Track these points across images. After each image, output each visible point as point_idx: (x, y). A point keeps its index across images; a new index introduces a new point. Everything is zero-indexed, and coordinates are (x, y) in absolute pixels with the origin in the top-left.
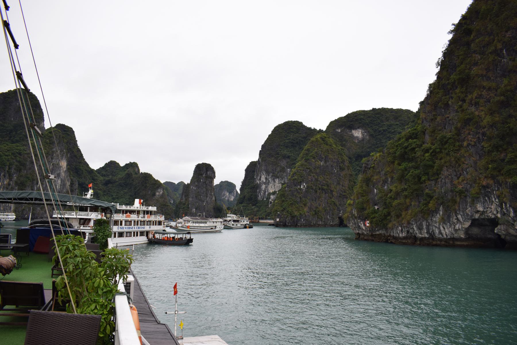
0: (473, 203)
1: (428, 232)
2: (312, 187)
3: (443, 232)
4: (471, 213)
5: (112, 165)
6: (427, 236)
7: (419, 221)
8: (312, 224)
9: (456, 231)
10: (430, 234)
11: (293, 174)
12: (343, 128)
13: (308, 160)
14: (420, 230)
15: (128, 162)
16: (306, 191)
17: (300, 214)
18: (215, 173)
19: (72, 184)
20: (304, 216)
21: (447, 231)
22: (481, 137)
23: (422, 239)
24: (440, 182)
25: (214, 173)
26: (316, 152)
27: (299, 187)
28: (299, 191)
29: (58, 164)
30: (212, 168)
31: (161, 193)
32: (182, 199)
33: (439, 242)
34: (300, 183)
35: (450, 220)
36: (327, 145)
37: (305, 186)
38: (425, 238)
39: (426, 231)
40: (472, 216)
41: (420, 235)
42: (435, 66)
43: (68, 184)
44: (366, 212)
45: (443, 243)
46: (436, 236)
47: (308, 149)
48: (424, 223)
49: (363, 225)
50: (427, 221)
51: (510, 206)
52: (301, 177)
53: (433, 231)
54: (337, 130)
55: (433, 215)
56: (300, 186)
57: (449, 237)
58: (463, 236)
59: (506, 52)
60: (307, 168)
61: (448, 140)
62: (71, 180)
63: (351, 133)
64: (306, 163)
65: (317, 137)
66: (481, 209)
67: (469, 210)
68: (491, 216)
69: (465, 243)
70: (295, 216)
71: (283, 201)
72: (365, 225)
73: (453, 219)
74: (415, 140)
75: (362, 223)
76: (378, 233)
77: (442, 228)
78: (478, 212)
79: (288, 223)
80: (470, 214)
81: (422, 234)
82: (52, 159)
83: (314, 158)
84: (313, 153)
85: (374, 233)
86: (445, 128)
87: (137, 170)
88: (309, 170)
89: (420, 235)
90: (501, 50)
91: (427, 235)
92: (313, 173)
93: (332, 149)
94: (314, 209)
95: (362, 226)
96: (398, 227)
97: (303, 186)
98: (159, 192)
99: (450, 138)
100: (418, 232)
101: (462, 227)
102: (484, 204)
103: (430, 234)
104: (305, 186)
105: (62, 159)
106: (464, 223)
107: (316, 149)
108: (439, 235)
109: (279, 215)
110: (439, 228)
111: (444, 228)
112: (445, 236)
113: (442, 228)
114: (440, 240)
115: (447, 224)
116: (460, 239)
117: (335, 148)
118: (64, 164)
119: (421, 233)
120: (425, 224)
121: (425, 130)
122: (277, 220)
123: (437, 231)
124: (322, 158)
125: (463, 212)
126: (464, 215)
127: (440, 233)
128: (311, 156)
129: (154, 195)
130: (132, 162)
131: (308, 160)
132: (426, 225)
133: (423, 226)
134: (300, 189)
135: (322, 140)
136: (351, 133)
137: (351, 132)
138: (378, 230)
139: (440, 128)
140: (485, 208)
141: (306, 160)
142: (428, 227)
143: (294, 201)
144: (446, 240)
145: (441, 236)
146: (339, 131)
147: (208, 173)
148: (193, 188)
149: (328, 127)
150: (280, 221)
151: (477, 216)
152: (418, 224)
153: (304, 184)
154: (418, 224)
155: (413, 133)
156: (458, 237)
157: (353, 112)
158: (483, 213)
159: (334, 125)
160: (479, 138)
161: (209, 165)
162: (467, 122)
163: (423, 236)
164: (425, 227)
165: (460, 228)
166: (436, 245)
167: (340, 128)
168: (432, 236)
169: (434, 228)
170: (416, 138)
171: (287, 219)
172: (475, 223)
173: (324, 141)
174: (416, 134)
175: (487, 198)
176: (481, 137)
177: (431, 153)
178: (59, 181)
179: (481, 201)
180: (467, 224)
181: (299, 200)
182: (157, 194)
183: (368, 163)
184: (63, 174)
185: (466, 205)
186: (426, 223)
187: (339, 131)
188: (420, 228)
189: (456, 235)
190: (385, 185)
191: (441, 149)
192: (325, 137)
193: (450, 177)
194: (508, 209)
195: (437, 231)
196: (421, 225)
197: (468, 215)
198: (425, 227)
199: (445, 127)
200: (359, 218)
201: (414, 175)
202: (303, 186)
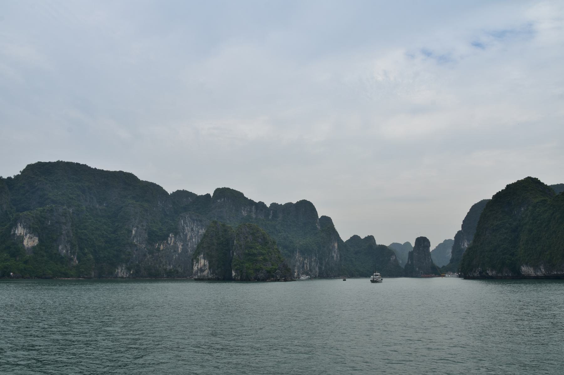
5: (355, 238)
15: (367, 236)
18: (430, 243)
19: (340, 257)
25: (429, 243)
29: (334, 246)
30: (428, 240)
31: (394, 258)
32: (408, 262)
43: (339, 256)
82: (331, 243)
98: (393, 258)
105: (335, 242)
118: (336, 245)
129: (390, 260)
130: (370, 235)
147: (425, 243)
148: (415, 254)
161: (425, 238)
178: (335, 255)
182: (392, 259)
184: (336, 251)
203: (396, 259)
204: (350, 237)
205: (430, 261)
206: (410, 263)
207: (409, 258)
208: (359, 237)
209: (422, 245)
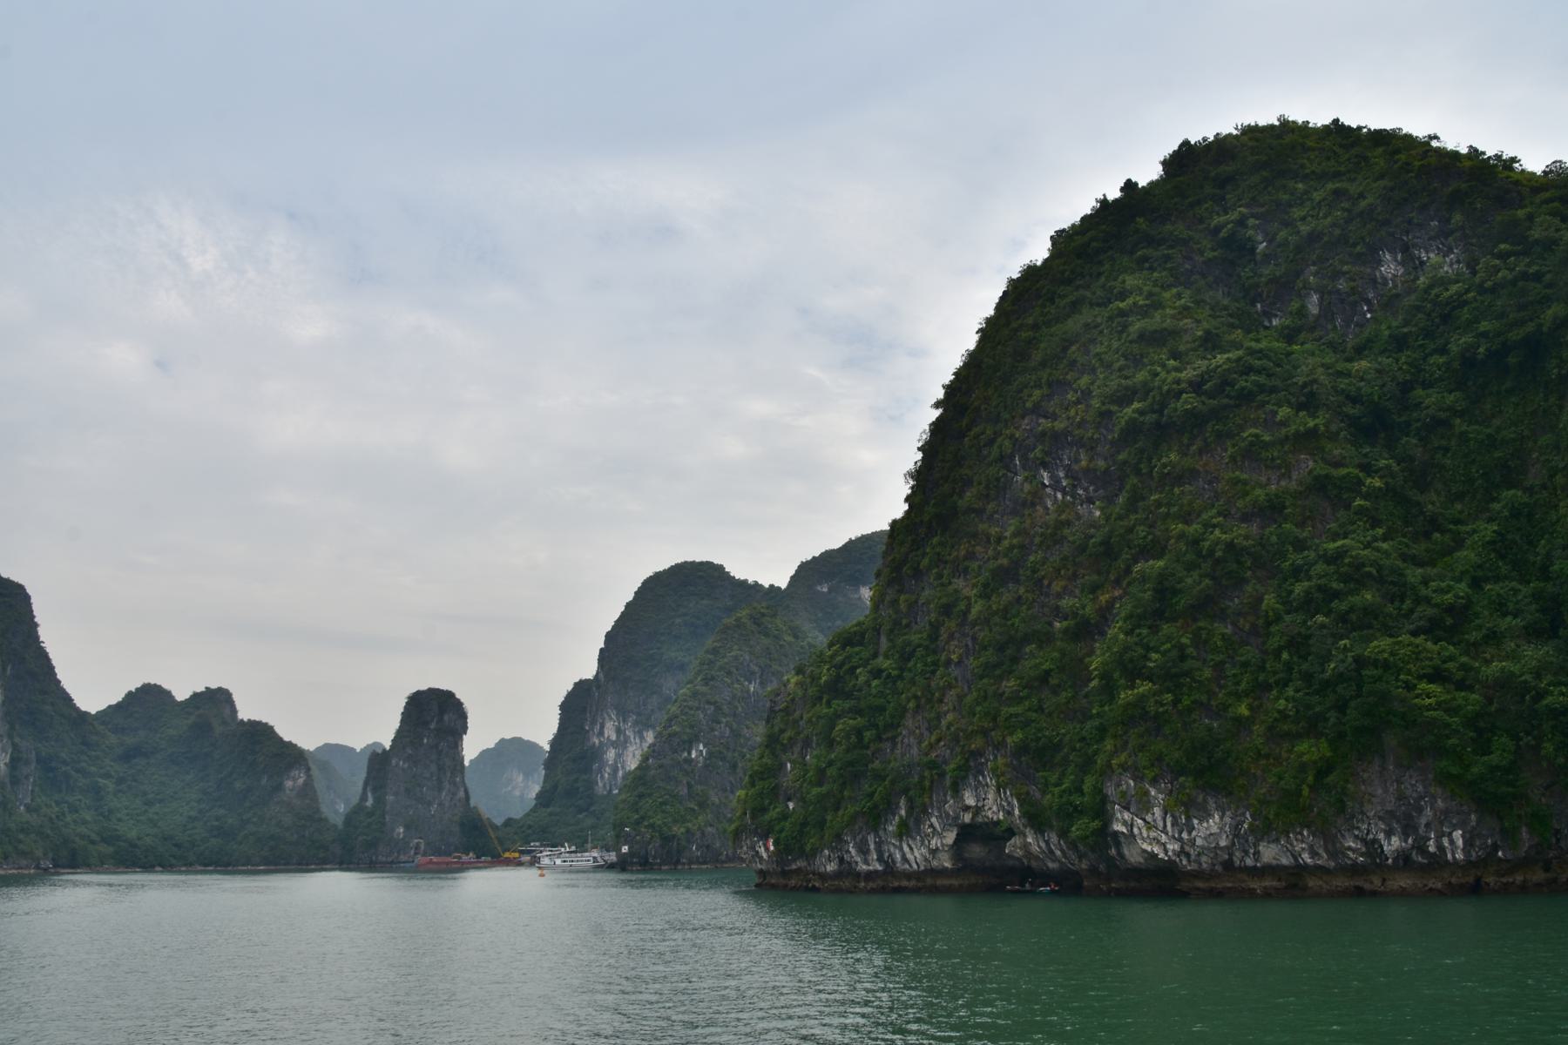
0: (956, 791)
1: (880, 859)
2: (720, 753)
3: (909, 856)
4: (954, 811)
5: (149, 698)
6: (880, 868)
7: (859, 834)
8: (723, 858)
9: (934, 852)
10: (886, 863)
11: (670, 720)
12: (834, 582)
13: (713, 678)
14: (865, 855)
15: (201, 689)
16: (706, 766)
17: (688, 831)
18: (466, 718)
20: (698, 834)
21: (913, 855)
22: (970, 643)
23: (870, 876)
24: (899, 745)
26: (736, 658)
27: (686, 754)
28: (686, 766)
30: (459, 704)
31: (301, 781)
32: (364, 798)
33: (905, 883)
34: (689, 744)
35: (920, 829)
36: (767, 635)
37: (701, 751)
38: (876, 872)
39: (875, 857)
40: (957, 817)
41: (864, 867)
42: (903, 479)
44: (767, 817)
45: (913, 883)
46: (897, 868)
47: (714, 649)
48: (871, 839)
49: (763, 849)
50: (877, 835)
51: (1011, 795)
52: (692, 727)
53: (890, 855)
54: (819, 588)
55: (886, 820)
56: (690, 753)
57: (922, 868)
58: (948, 865)
59: (1020, 462)
60: (709, 703)
61: (914, 650)
62: (15, 746)
63: (856, 596)
64: (704, 689)
65: (739, 615)
66: (971, 801)
67: (950, 804)
68: (990, 816)
69: (955, 882)
70: (674, 836)
71: (641, 796)
72: (767, 849)
73: (924, 825)
74: (857, 649)
75: (761, 843)
76: (794, 867)
77: (906, 848)
78: (967, 808)
79: (655, 858)
80: (951, 813)
81: (869, 865)
83: (729, 673)
84: (726, 660)
85: (786, 868)
86: (916, 623)
87: (227, 711)
88: (712, 708)
89: (864, 867)
90: (1012, 457)
91: (880, 865)
92: (725, 715)
93: (781, 646)
94: (729, 815)
95: (762, 850)
96: (822, 850)
97: (698, 752)
98: (295, 779)
99: (919, 646)
100: (859, 859)
101: (943, 845)
102: (976, 791)
103: (886, 863)
104: (701, 751)
106: (944, 834)
107: (736, 647)
108: (903, 864)
109: (628, 834)
110: (901, 849)
111: (911, 849)
112: (915, 866)
113: (906, 848)
114: (908, 875)
115: (915, 839)
116: (943, 872)
117: (790, 644)
119: (866, 862)
120: (873, 840)
121: (880, 627)
122: (623, 851)
123: (898, 856)
124: (753, 673)
125: (939, 809)
126: (941, 815)
127: (905, 859)
128: (721, 668)
129: (279, 787)
130: (214, 686)
131: (713, 678)
132: (875, 842)
133: (869, 845)
134: (689, 761)
135: (755, 623)
136: (856, 596)
137: (857, 590)
138: (794, 860)
139: (904, 622)
140: (978, 801)
141: (706, 681)
142: (880, 846)
143: (670, 795)
144: (918, 875)
145: (908, 867)
146: (825, 590)
147: (446, 718)
148: (397, 765)
149: (792, 578)
150: (631, 854)
151: (967, 818)
152: (858, 840)
153: (701, 747)
154: (858, 840)
155: (855, 633)
156: (941, 867)
157: (863, 536)
158: (978, 810)
159: (810, 572)
160: (967, 645)
161: (449, 695)
162: (947, 610)
163: (871, 868)
164: (872, 847)
165: (939, 845)
166: (899, 890)
167: (826, 582)
168: (890, 868)
169: (892, 849)
170: (861, 644)
171: (650, 847)
172: (967, 834)
173: (759, 625)
174: (862, 635)
175: (981, 778)
176: (970, 643)
177: (885, 679)
179: (970, 785)
180: (950, 837)
181: (686, 791)
182: (289, 784)
183: (776, 699)
185: (945, 795)
186: (875, 838)
187: (825, 590)
188: (864, 851)
189: (935, 863)
190: (807, 751)
191: (902, 669)
192: (763, 615)
193: (917, 731)
194: (1010, 799)
195: (898, 856)
196: (864, 842)
197: (948, 815)
198: (872, 847)
199: (915, 618)
200: (756, 833)
201: (848, 729)
202: (698, 752)
203: (309, 784)
204: (126, 692)
205: (461, 794)
206: (370, 802)
207: (366, 784)
208: (168, 694)
209: (433, 726)
